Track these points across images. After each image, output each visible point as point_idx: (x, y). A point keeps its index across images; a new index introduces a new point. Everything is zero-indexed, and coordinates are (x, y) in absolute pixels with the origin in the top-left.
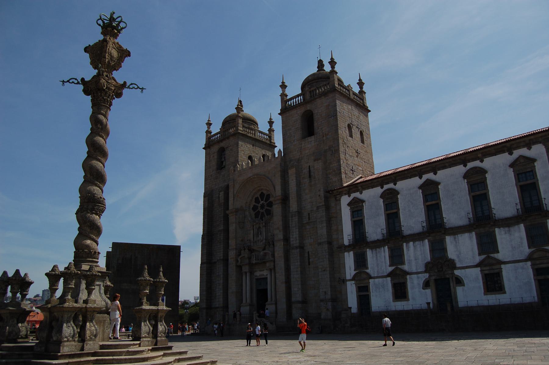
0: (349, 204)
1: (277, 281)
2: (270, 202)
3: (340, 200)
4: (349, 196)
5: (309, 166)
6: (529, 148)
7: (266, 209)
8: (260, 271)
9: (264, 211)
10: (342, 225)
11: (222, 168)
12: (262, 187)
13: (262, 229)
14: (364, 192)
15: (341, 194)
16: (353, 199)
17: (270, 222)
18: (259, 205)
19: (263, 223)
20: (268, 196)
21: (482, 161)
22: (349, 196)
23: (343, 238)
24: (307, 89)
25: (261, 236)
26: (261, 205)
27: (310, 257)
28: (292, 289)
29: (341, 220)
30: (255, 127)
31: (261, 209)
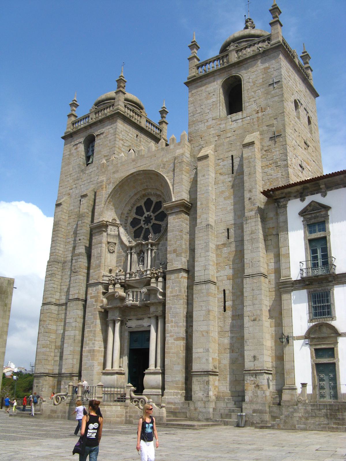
1: (167, 335)
3: (285, 207)
4: (303, 200)
5: (232, 156)
7: (154, 223)
8: (138, 319)
9: (149, 226)
10: (289, 246)
11: (87, 165)
12: (150, 190)
13: (146, 254)
14: (329, 193)
15: (288, 197)
16: (310, 205)
17: (159, 244)
18: (143, 218)
19: (147, 244)
20: (159, 205)
22: (303, 200)
23: (290, 268)
24: (232, 47)
26: (145, 217)
27: (226, 300)
28: (194, 350)
30: (141, 112)
31: (144, 224)
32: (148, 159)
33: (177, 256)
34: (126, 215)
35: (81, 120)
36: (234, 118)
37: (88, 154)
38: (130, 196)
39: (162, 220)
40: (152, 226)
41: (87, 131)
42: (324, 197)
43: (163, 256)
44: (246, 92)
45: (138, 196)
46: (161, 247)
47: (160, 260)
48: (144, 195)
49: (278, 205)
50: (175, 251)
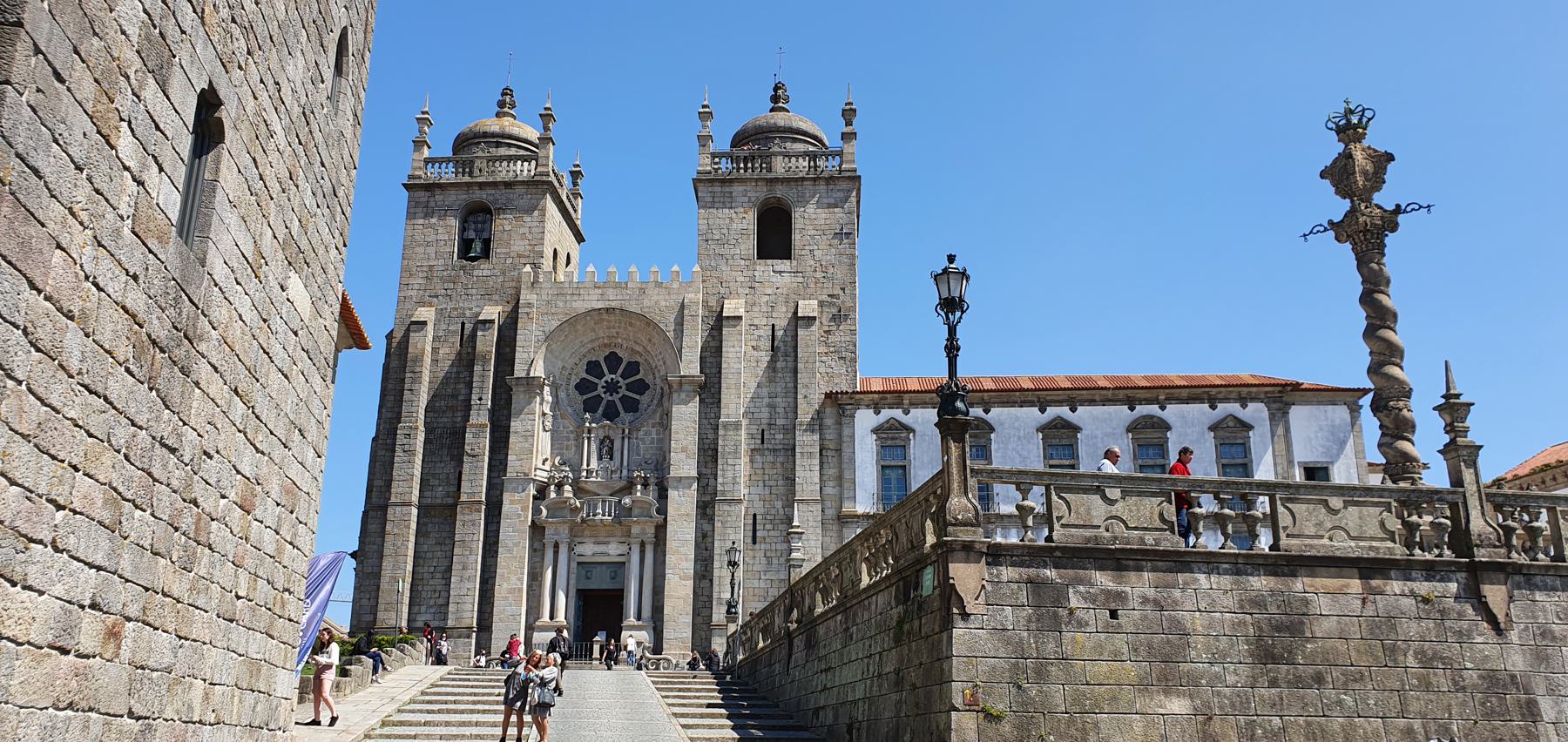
0: (875, 431)
2: (642, 380)
4: (877, 413)
5: (773, 325)
6: (1244, 406)
13: (617, 445)
15: (857, 405)
21: (1163, 408)
22: (877, 413)
25: (611, 459)
29: (852, 460)
31: (605, 393)
33: (688, 457)
36: (778, 268)
37: (465, 233)
41: (471, 192)
42: (906, 414)
44: (797, 231)
45: (596, 344)
48: (605, 345)
49: (844, 413)
50: (684, 450)
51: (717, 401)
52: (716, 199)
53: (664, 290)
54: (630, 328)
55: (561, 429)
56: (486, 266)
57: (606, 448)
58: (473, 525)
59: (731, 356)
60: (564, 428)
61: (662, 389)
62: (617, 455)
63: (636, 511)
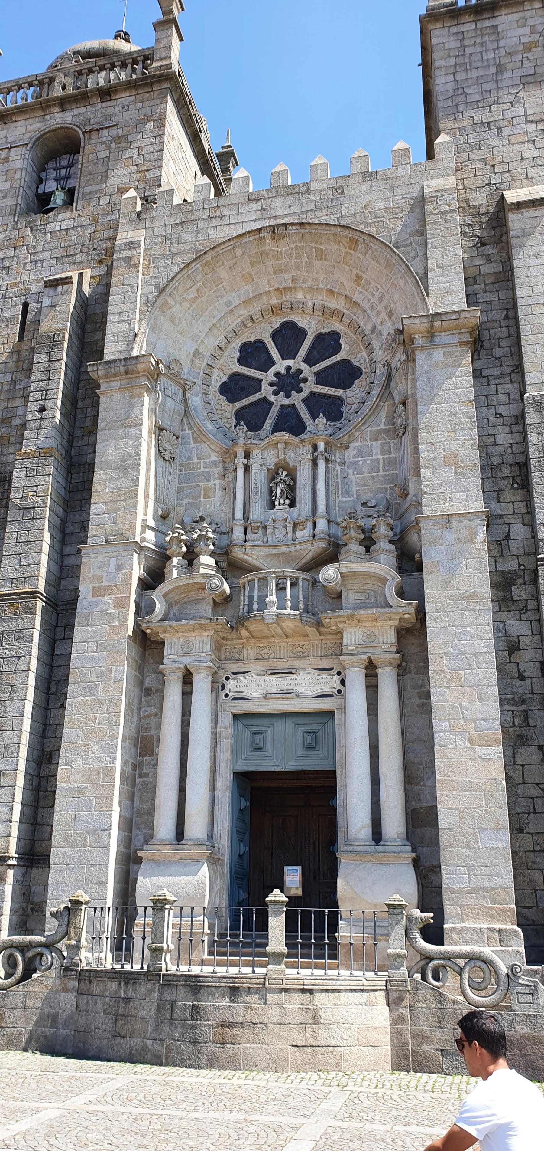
2: (345, 363)
7: (312, 393)
17: (347, 448)
26: (277, 375)
31: (276, 393)
32: (312, 197)
34: (207, 360)
35: (20, 87)
38: (228, 304)
39: (346, 385)
40: (305, 401)
41: (48, 117)
43: (365, 486)
45: (254, 309)
46: (355, 456)
47: (355, 496)
51: (509, 370)
52: (466, 42)
53: (381, 183)
54: (317, 264)
55: (195, 460)
56: (67, 215)
57: (282, 486)
58: (19, 639)
59: (533, 272)
60: (198, 459)
61: (389, 365)
62: (303, 494)
63: (350, 598)
